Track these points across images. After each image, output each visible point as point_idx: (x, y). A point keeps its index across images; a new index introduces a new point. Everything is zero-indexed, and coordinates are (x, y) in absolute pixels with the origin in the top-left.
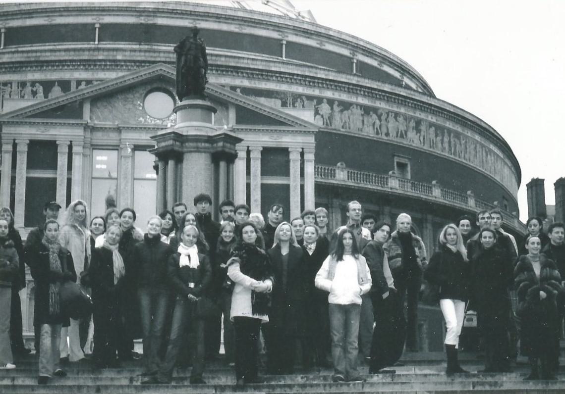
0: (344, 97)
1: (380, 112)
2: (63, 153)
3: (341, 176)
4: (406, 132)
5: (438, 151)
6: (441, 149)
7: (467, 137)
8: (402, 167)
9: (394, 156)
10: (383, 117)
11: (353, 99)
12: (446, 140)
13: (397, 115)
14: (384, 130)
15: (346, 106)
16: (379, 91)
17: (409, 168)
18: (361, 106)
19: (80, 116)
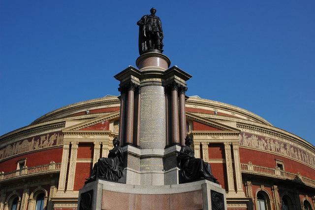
0: (248, 131)
1: (266, 138)
2: (97, 149)
3: (251, 169)
4: (280, 149)
5: (296, 159)
6: (298, 158)
7: (308, 154)
8: (280, 166)
9: (275, 160)
10: (268, 141)
11: (252, 132)
12: (299, 154)
13: (274, 141)
14: (269, 148)
15: (249, 135)
16: (265, 128)
17: (283, 166)
18: (257, 136)
19: (108, 129)
